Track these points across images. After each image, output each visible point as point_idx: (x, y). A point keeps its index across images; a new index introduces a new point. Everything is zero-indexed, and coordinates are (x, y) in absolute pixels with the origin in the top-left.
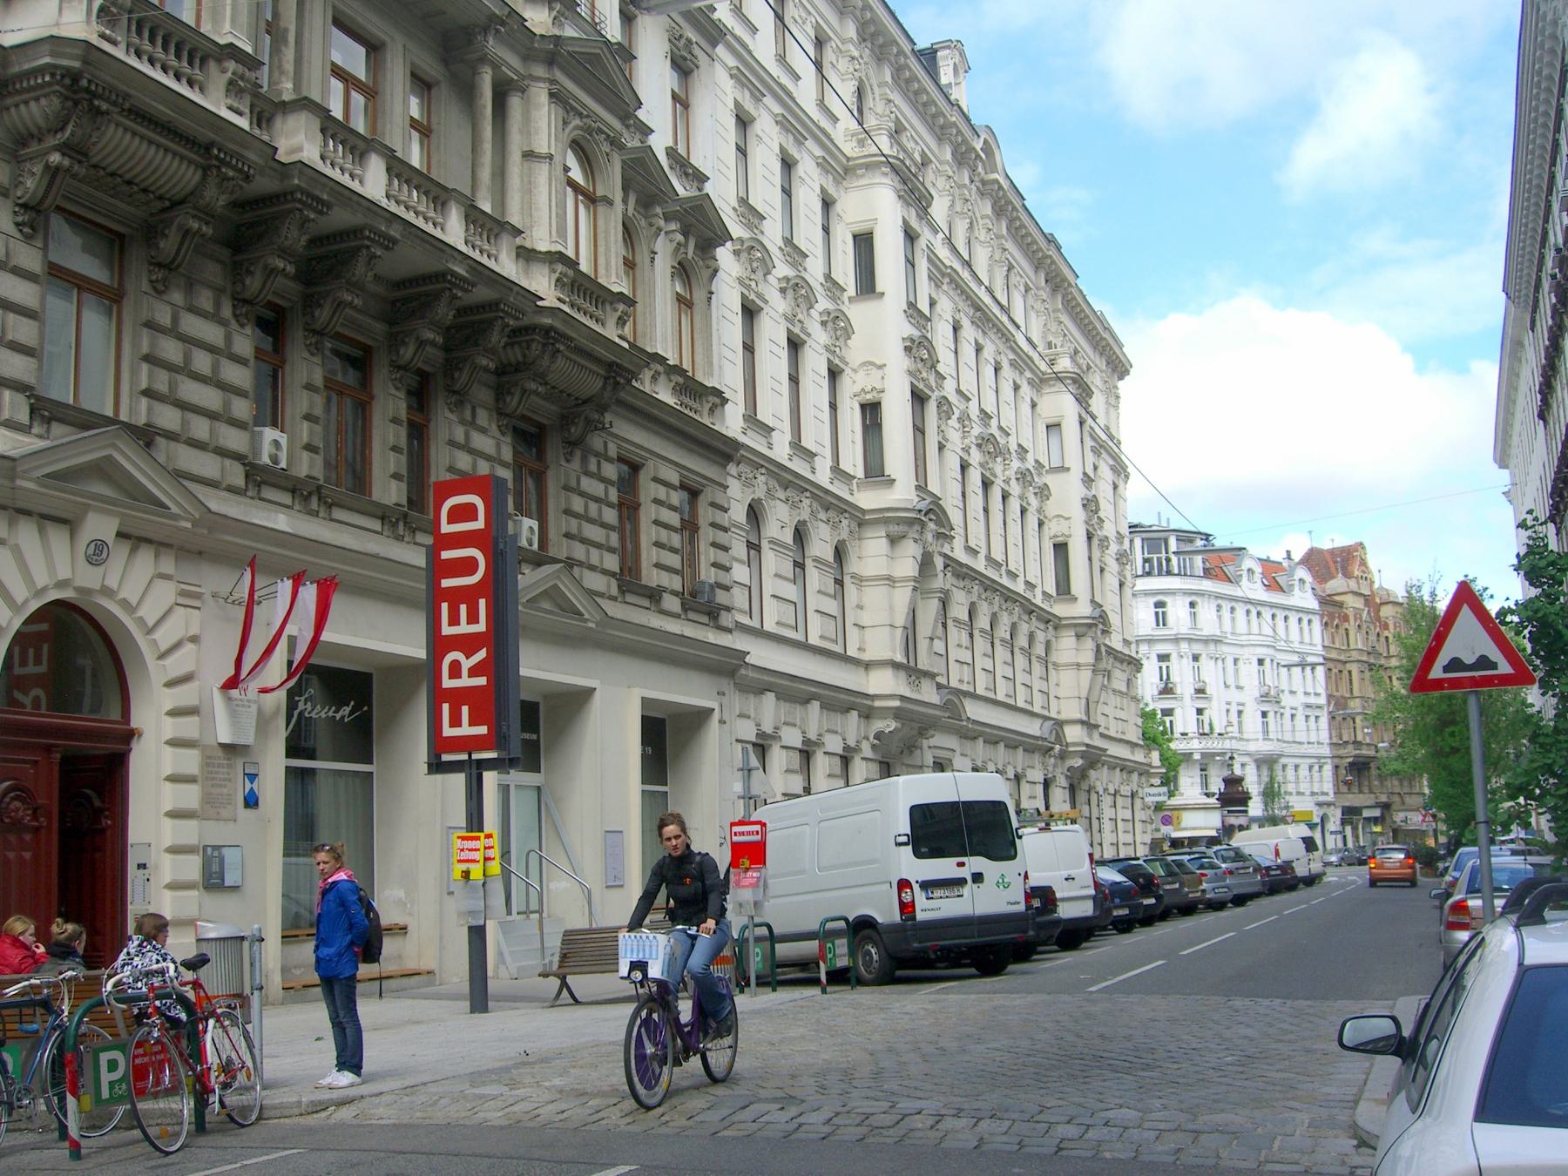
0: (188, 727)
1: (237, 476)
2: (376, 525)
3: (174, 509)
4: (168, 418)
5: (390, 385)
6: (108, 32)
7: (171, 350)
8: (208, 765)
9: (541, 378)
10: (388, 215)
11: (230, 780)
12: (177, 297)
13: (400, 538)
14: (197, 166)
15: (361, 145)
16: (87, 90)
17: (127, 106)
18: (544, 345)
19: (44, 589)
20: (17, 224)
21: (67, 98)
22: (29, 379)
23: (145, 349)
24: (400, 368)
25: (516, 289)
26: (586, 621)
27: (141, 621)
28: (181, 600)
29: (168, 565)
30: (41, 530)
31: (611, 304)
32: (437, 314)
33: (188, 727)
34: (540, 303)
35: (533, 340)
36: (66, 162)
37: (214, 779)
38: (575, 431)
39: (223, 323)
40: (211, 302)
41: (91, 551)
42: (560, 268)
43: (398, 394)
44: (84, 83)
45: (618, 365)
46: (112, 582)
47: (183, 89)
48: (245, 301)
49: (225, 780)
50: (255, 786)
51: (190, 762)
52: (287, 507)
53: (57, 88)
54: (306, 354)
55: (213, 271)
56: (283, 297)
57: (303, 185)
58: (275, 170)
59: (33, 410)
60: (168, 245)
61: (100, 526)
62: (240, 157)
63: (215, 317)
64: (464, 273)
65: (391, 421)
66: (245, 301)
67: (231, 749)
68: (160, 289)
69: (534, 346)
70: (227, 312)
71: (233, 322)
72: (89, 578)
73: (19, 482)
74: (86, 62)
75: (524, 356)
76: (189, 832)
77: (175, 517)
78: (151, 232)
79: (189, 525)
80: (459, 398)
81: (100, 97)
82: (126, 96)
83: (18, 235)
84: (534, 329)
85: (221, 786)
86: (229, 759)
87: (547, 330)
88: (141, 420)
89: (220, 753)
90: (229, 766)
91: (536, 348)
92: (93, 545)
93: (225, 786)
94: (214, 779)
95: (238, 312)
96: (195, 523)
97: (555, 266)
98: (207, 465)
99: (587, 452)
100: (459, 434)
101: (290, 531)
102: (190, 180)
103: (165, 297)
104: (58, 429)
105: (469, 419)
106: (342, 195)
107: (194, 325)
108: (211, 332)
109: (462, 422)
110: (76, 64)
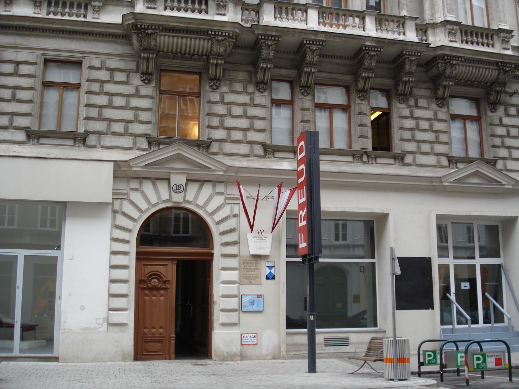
1: (259, 150)
2: (350, 159)
3: (213, 168)
4: (220, 134)
5: (357, 99)
6: (149, 6)
7: (221, 109)
8: (244, 263)
9: (449, 78)
10: (314, 32)
11: (258, 269)
12: (225, 89)
13: (364, 163)
14: (208, 40)
15: (303, 8)
16: (141, 28)
17: (161, 28)
18: (446, 63)
19: (156, 204)
20: (142, 81)
21: (139, 34)
22: (148, 132)
23: (207, 112)
24: (360, 91)
25: (410, 43)
26: (504, 185)
27: (206, 212)
28: (227, 201)
29: (220, 188)
30: (154, 184)
31: (498, 35)
32: (365, 65)
34: (430, 46)
35: (438, 63)
36: (146, 55)
37: (248, 269)
38: (493, 97)
39: (252, 93)
40: (242, 87)
41: (175, 187)
42: (448, 27)
43: (363, 102)
44: (139, 26)
45: (502, 62)
46: (190, 197)
47: (196, 16)
48: (260, 83)
49: (255, 269)
50: (273, 271)
51: (233, 263)
53: (133, 31)
54: (302, 97)
55: (242, 75)
56: (289, 77)
57: (260, 32)
58: (248, 31)
59: (150, 144)
60: (212, 71)
61: (179, 179)
62: (222, 31)
63: (245, 92)
64: (374, 44)
65: (358, 114)
66: (260, 83)
67: (258, 257)
68: (215, 88)
69: (440, 65)
70: (251, 89)
71: (257, 93)
72: (178, 198)
73: (133, 169)
74: (136, 19)
75: (438, 70)
76: (233, 289)
77: (214, 171)
78: (207, 68)
79: (222, 173)
80: (404, 97)
81: (148, 29)
82: (159, 26)
83: (143, 84)
84: (436, 58)
87: (443, 56)
88: (205, 138)
89: (250, 259)
90: (256, 263)
91: (441, 66)
92: (175, 186)
93: (254, 271)
94: (248, 269)
95: (258, 88)
96: (225, 172)
97: (446, 27)
98: (244, 149)
99: (507, 105)
100: (406, 112)
101: (291, 168)
102: (207, 46)
103: (218, 90)
104: (161, 146)
105: (413, 105)
106: (284, 31)
107: (230, 98)
108: (245, 99)
109: (409, 106)
110: (133, 21)
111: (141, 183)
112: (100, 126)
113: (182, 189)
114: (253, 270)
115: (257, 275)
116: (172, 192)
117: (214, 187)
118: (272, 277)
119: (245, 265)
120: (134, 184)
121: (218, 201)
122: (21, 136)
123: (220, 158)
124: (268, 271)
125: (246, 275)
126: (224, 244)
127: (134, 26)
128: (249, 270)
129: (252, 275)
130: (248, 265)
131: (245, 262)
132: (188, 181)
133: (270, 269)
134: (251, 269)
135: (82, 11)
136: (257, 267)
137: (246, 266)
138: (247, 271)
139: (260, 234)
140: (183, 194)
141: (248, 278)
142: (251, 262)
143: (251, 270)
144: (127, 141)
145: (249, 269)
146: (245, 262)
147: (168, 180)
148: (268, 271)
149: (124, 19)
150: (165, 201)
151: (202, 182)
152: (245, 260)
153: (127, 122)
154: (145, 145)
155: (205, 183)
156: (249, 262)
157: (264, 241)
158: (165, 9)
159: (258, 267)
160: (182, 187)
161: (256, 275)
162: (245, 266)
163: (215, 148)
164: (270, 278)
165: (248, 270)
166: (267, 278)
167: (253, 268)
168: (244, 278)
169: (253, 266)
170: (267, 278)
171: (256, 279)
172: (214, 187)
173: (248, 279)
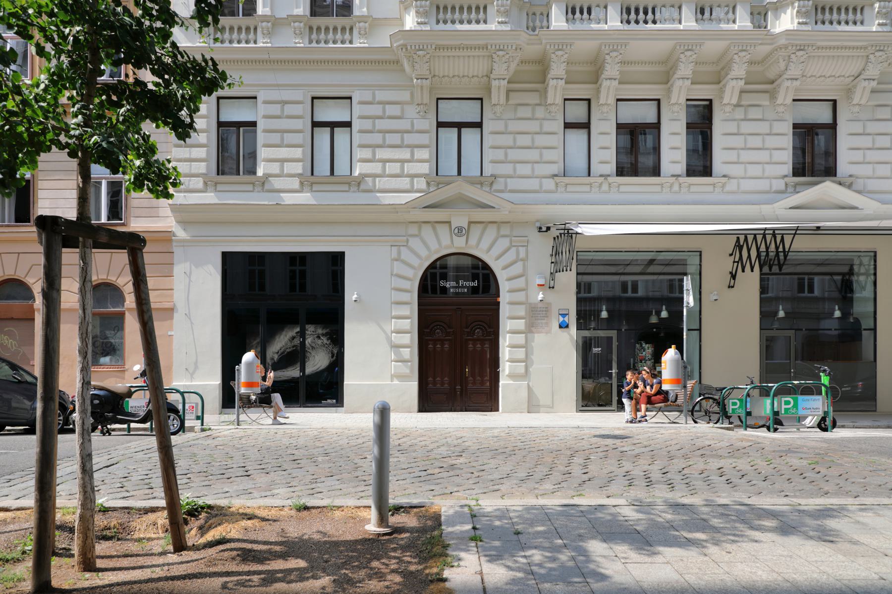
0: (520, 297)
8: (532, 311)
11: (547, 317)
29: (505, 230)
30: (434, 229)
33: (520, 297)
41: (456, 231)
50: (566, 319)
52: (588, 192)
59: (428, 184)
79: (507, 213)
85: (542, 319)
90: (546, 311)
92: (457, 229)
93: (544, 320)
104: (440, 186)
111: (420, 229)
112: (375, 168)
113: (464, 231)
116: (454, 235)
117: (499, 229)
118: (566, 325)
120: (413, 230)
121: (503, 243)
122: (295, 183)
123: (506, 195)
124: (561, 319)
126: (510, 291)
127: (404, 47)
132: (470, 223)
134: (541, 317)
135: (347, 36)
140: (465, 237)
144: (404, 183)
145: (537, 317)
147: (449, 223)
148: (561, 319)
149: (392, 40)
150: (447, 247)
151: (486, 224)
153: (403, 161)
154: (423, 186)
155: (490, 225)
158: (438, 22)
160: (464, 230)
163: (499, 185)
166: (560, 327)
169: (542, 314)
170: (560, 327)
172: (499, 229)
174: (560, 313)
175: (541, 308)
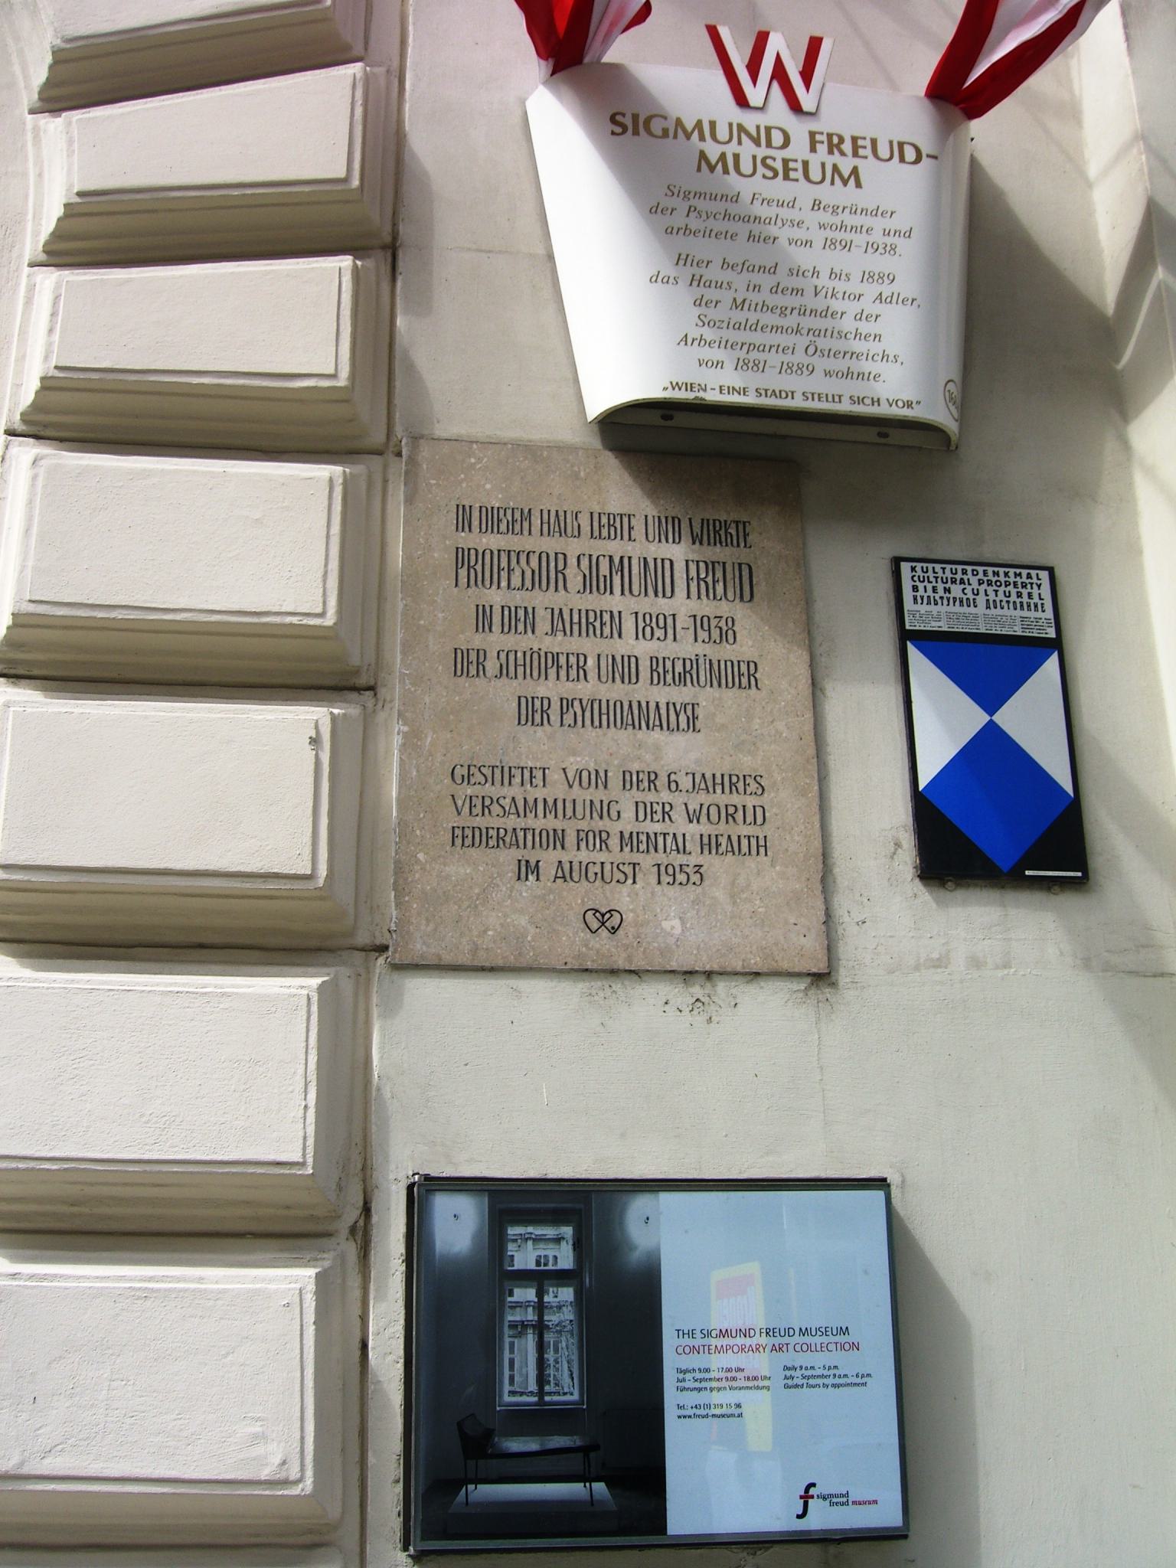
11: (744, 675)
37: (547, 664)
85: (641, 717)
86: (708, 533)
93: (689, 719)
94: (547, 664)
114: (662, 695)
115: (732, 783)
119: (496, 597)
125: (506, 774)
128: (584, 690)
129: (629, 780)
130: (541, 600)
131: (493, 541)
133: (990, 697)
134: (624, 669)
136: (727, 633)
137: (520, 620)
138: (532, 712)
139: (755, 94)
141: (557, 839)
142: (616, 548)
143: (617, 691)
146: (493, 541)
152: (492, 519)
156: (573, 547)
157: (835, 194)
159: (743, 648)
161: (705, 783)
162: (483, 618)
164: (1005, 865)
165: (551, 689)
167: (644, 649)
168: (465, 838)
169: (651, 625)
171: (714, 865)
173: (549, 859)
174: (923, 615)
175: (615, 525)
